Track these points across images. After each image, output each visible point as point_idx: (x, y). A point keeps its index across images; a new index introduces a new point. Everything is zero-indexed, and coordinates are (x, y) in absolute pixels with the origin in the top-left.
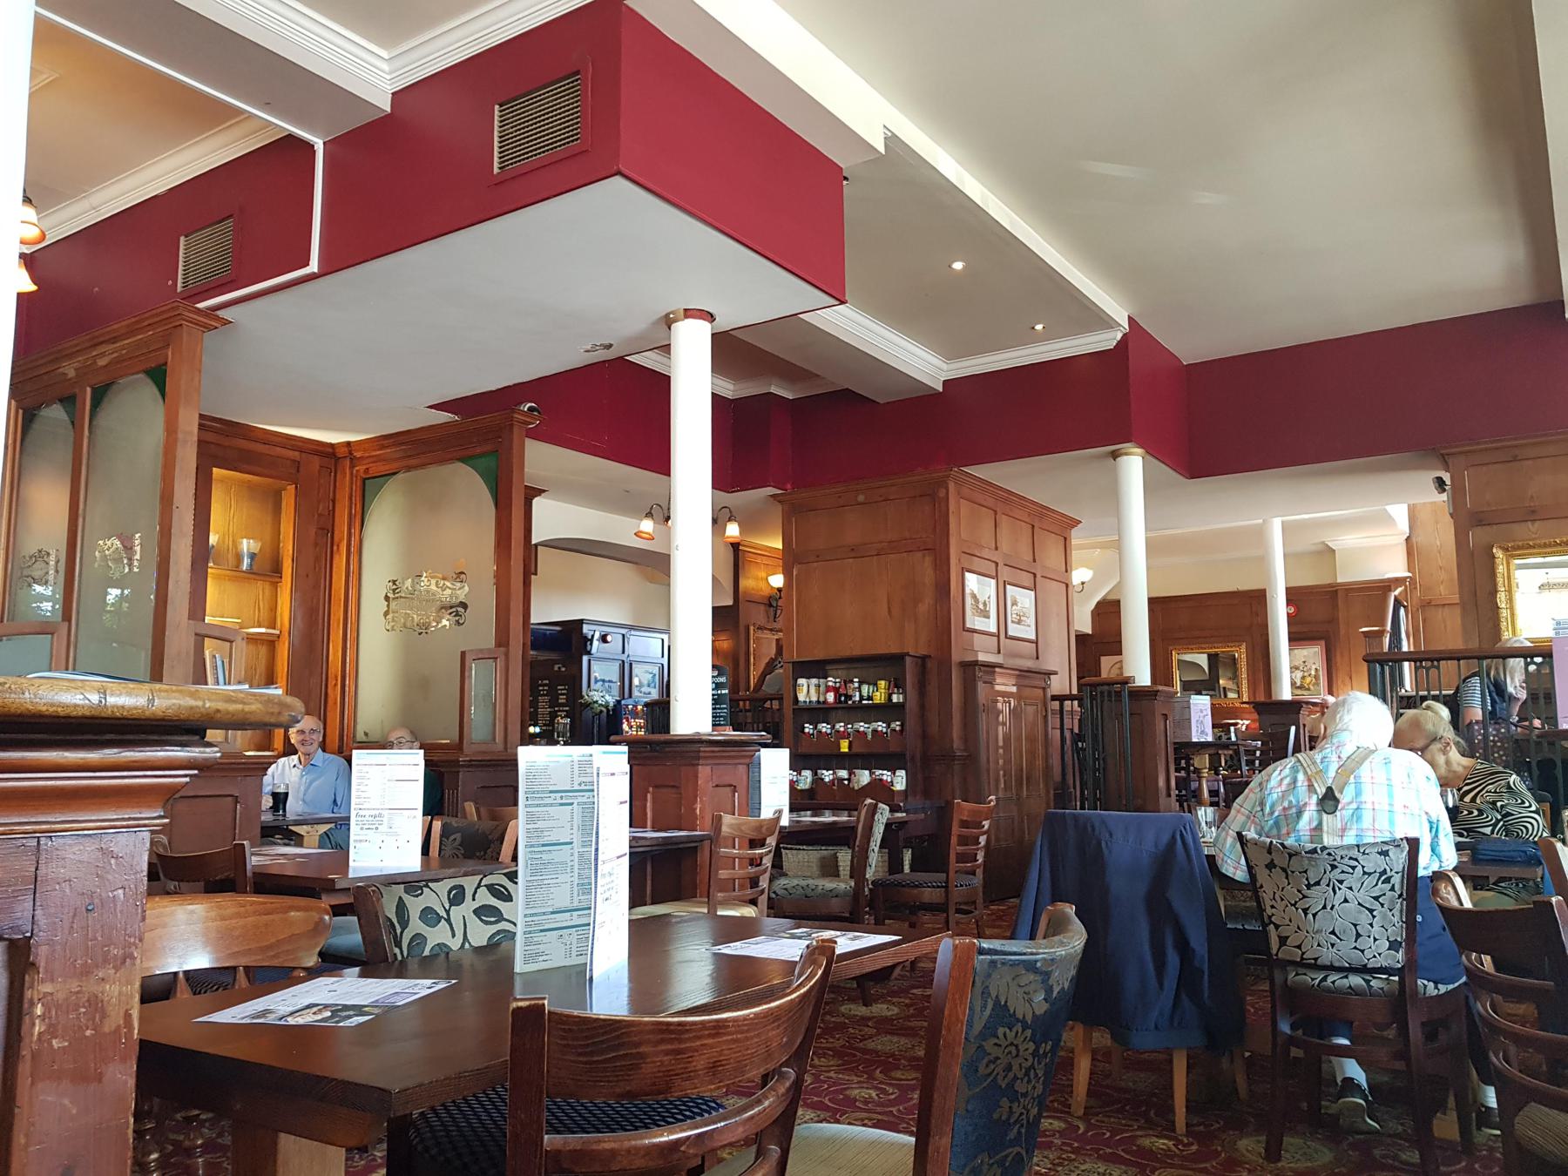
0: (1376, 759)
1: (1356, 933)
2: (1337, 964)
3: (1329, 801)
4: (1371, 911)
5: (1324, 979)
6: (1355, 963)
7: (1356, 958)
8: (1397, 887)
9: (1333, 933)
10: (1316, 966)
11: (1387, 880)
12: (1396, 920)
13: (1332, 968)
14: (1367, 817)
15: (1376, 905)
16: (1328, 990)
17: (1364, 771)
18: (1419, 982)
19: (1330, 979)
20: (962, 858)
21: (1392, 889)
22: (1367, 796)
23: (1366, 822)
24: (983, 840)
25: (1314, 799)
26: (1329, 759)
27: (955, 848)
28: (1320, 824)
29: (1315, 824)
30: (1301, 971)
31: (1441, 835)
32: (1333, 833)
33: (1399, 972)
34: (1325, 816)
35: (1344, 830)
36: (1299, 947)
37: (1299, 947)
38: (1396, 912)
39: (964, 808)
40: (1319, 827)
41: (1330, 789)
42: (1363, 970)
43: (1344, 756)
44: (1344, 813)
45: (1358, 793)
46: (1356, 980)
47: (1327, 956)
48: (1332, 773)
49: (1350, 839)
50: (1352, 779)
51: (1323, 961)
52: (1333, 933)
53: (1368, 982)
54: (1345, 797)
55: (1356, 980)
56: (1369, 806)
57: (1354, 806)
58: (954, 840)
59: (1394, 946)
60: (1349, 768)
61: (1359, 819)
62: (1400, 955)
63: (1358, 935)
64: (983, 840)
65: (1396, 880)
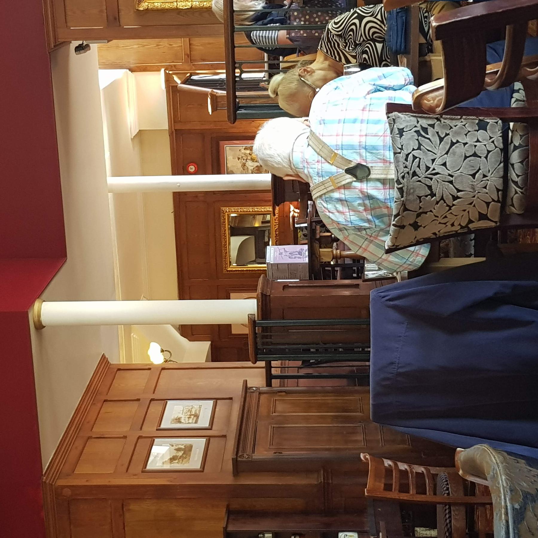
0: (318, 130)
1: (470, 157)
2: (502, 173)
3: (359, 172)
4: (453, 144)
5: (516, 183)
6: (501, 158)
7: (495, 157)
8: (431, 122)
9: (473, 176)
10: (505, 190)
11: (425, 130)
12: (459, 124)
14: (371, 141)
15: (448, 140)
16: (525, 181)
17: (331, 141)
18: (514, 106)
19: (516, 179)
20: (421, 490)
21: (433, 126)
22: (355, 141)
23: (378, 142)
24: (403, 466)
25: (357, 184)
26: (315, 169)
27: (412, 496)
28: (378, 180)
29: (379, 185)
30: (509, 202)
31: (385, 82)
32: (387, 169)
33: (505, 122)
34: (372, 176)
35: (385, 161)
36: (488, 204)
37: (488, 204)
38: (452, 123)
39: (372, 486)
40: (383, 182)
41: (349, 171)
43: (316, 157)
44: (369, 160)
45: (351, 147)
46: (515, 157)
47: (494, 180)
48: (334, 169)
49: (390, 155)
50: (340, 152)
52: (473, 176)
53: (516, 148)
54: (355, 159)
56: (363, 139)
57: (363, 151)
58: (404, 497)
59: (483, 126)
60: (330, 155)
61: (374, 148)
62: (490, 121)
63: (475, 155)
64: (403, 466)
65: (424, 123)
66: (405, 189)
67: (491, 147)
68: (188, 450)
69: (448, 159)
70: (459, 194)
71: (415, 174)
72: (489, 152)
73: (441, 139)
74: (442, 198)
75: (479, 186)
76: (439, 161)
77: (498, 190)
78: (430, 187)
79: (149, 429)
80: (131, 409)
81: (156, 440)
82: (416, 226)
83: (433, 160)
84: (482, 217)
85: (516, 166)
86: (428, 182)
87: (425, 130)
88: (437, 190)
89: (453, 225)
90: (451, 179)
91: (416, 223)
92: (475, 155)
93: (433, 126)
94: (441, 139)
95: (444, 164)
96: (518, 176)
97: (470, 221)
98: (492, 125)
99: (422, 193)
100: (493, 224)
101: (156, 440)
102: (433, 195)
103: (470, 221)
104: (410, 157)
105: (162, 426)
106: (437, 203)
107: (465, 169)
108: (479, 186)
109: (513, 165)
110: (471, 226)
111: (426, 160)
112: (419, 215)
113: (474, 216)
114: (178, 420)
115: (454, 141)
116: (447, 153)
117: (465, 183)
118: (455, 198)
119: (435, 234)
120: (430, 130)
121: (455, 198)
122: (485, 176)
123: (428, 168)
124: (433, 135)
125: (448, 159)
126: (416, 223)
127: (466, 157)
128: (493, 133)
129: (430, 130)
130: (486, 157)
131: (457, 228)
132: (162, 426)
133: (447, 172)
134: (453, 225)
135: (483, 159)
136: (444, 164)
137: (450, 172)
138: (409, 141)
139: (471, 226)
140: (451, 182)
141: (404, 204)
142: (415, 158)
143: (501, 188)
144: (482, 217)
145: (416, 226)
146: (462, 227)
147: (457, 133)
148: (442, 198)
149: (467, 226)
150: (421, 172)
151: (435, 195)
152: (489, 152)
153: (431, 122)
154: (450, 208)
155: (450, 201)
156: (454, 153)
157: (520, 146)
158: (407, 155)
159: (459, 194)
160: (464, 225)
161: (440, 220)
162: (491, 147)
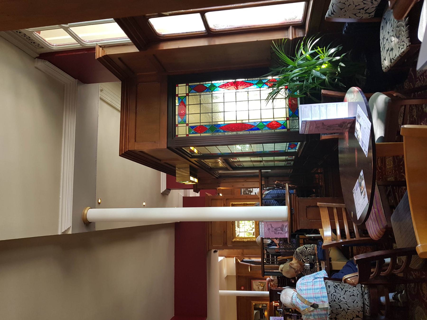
4: (346, 291)
5: (367, 305)
6: (362, 297)
8: (338, 284)
13: (364, 303)
47: (360, 304)
51: (362, 305)
52: (354, 302)
53: (366, 293)
55: (366, 296)
63: (353, 295)
67: (358, 293)
69: (345, 296)
71: (335, 301)
73: (342, 290)
75: (356, 306)
78: (340, 306)
85: (367, 299)
87: (337, 286)
88: (342, 306)
92: (353, 295)
93: (339, 285)
94: (342, 290)
95: (344, 298)
102: (341, 308)
107: (350, 300)
108: (356, 306)
111: (338, 296)
112: (337, 315)
117: (351, 305)
118: (348, 309)
120: (338, 286)
121: (348, 309)
123: (339, 299)
125: (345, 296)
129: (338, 286)
133: (345, 301)
136: (344, 298)
138: (332, 290)
141: (332, 311)
142: (334, 295)
147: (347, 288)
148: (344, 309)
150: (336, 300)
153: (338, 284)
157: (367, 293)
162: (358, 293)
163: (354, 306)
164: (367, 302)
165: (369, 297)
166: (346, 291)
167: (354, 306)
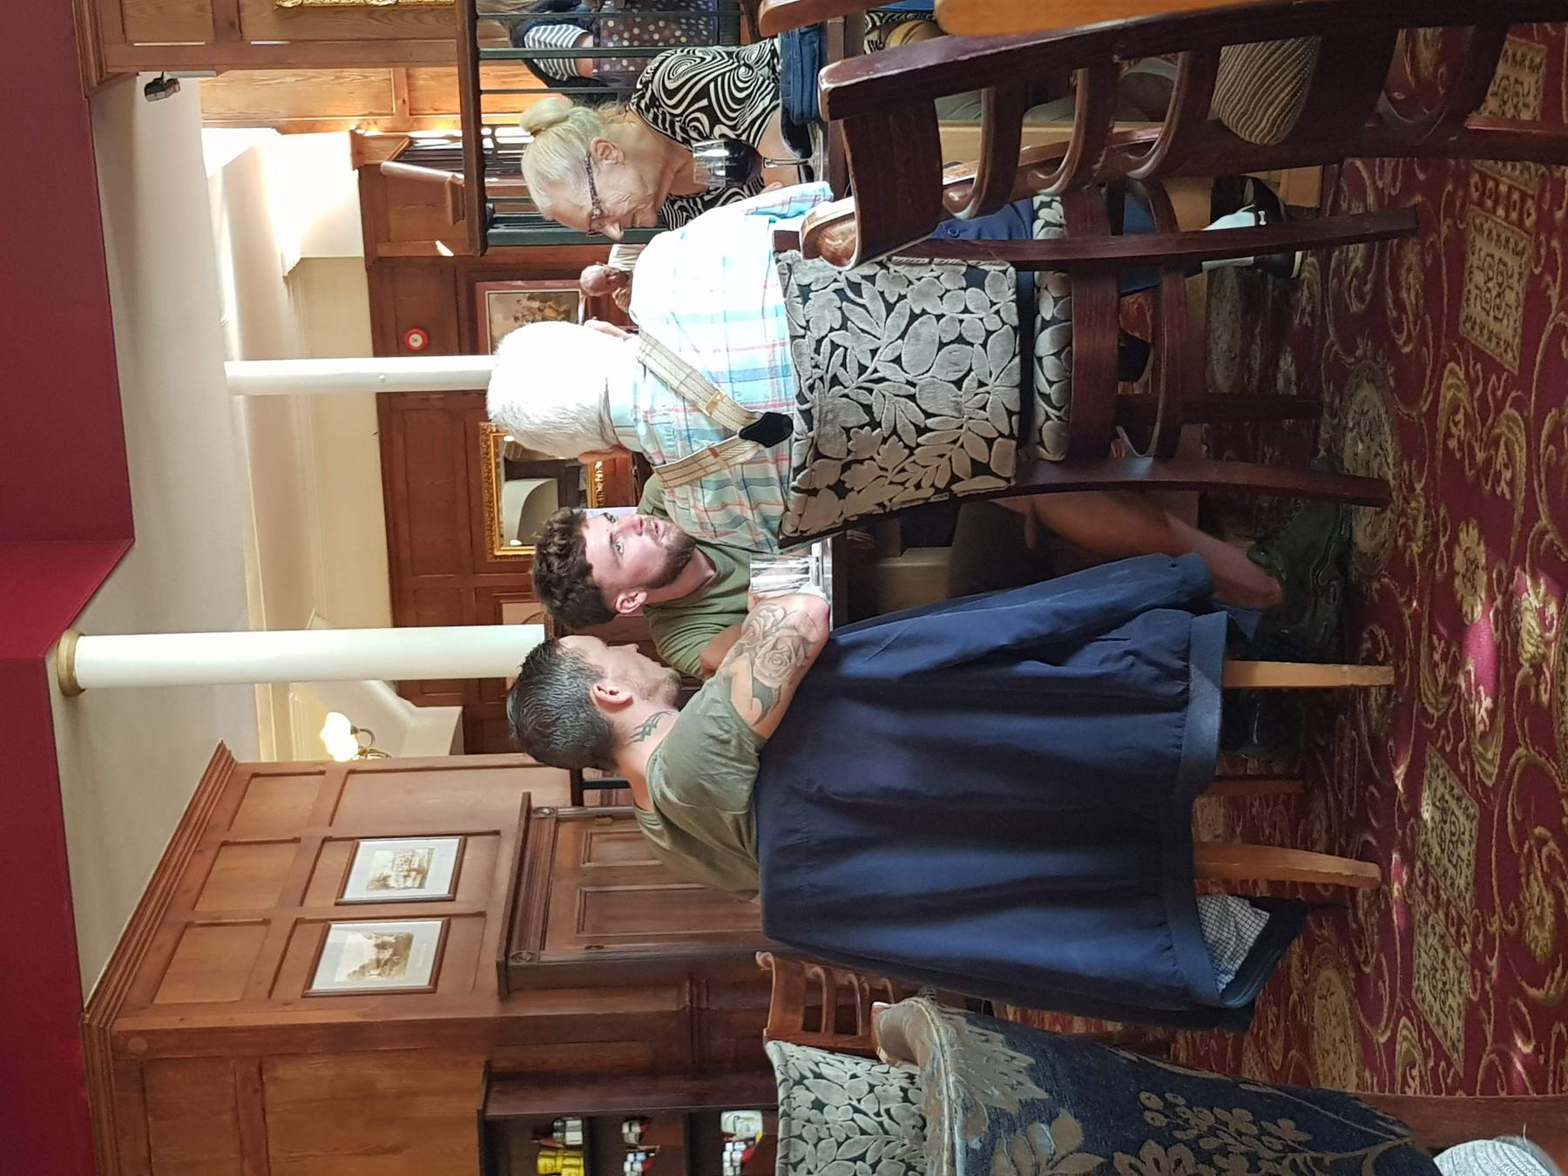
2: (1016, 378)
4: (914, 317)
5: (1046, 397)
6: (1013, 345)
7: (1004, 343)
9: (958, 383)
12: (927, 275)
18: (1041, 236)
19: (1045, 388)
37: (990, 442)
38: (913, 273)
42: (1026, 332)
46: (1045, 343)
47: (1002, 393)
52: (958, 383)
53: (1046, 324)
59: (975, 279)
62: (992, 268)
63: (960, 340)
66: (815, 412)
67: (993, 323)
68: (403, 946)
69: (906, 349)
70: (930, 422)
72: (989, 333)
73: (890, 308)
74: (894, 432)
76: (886, 354)
77: (1010, 413)
78: (868, 409)
79: (319, 903)
80: (279, 861)
81: (334, 926)
82: (840, 490)
83: (874, 352)
84: (979, 469)
86: (864, 398)
87: (856, 288)
89: (918, 486)
90: (913, 390)
91: (841, 482)
92: (960, 340)
93: (871, 279)
94: (890, 308)
95: (897, 360)
96: (1051, 384)
97: (955, 479)
98: (994, 277)
99: (852, 421)
100: (1002, 484)
101: (334, 926)
102: (875, 424)
103: (955, 479)
104: (826, 342)
105: (349, 896)
106: (885, 441)
107: (943, 373)
109: (1040, 359)
110: (954, 487)
111: (859, 351)
112: (846, 467)
113: (962, 467)
114: (383, 882)
115: (917, 311)
116: (902, 337)
117: (941, 400)
118: (921, 431)
119: (881, 505)
120: (866, 286)
121: (921, 431)
122: (981, 384)
123: (863, 369)
124: (872, 299)
125: (906, 349)
126: (841, 482)
127: (942, 345)
128: (996, 293)
129: (866, 286)
130: (984, 345)
131: (927, 492)
132: (349, 896)
134: (918, 486)
135: (978, 347)
137: (910, 377)
138: (823, 312)
139: (954, 487)
140: (912, 397)
141: (814, 445)
142: (834, 346)
143: (1015, 407)
144: (979, 469)
145: (840, 490)
146: (938, 491)
148: (894, 432)
149: (947, 488)
150: (849, 377)
151: (879, 425)
152: (989, 333)
154: (912, 450)
155: (910, 437)
156: (917, 336)
157: (1054, 321)
158: (819, 342)
159: (930, 422)
160: (942, 485)
161: (891, 476)
162: (993, 323)
163: (958, 407)
164: (1047, 375)
165: (1063, 348)
166: (914, 317)
167: (958, 407)
